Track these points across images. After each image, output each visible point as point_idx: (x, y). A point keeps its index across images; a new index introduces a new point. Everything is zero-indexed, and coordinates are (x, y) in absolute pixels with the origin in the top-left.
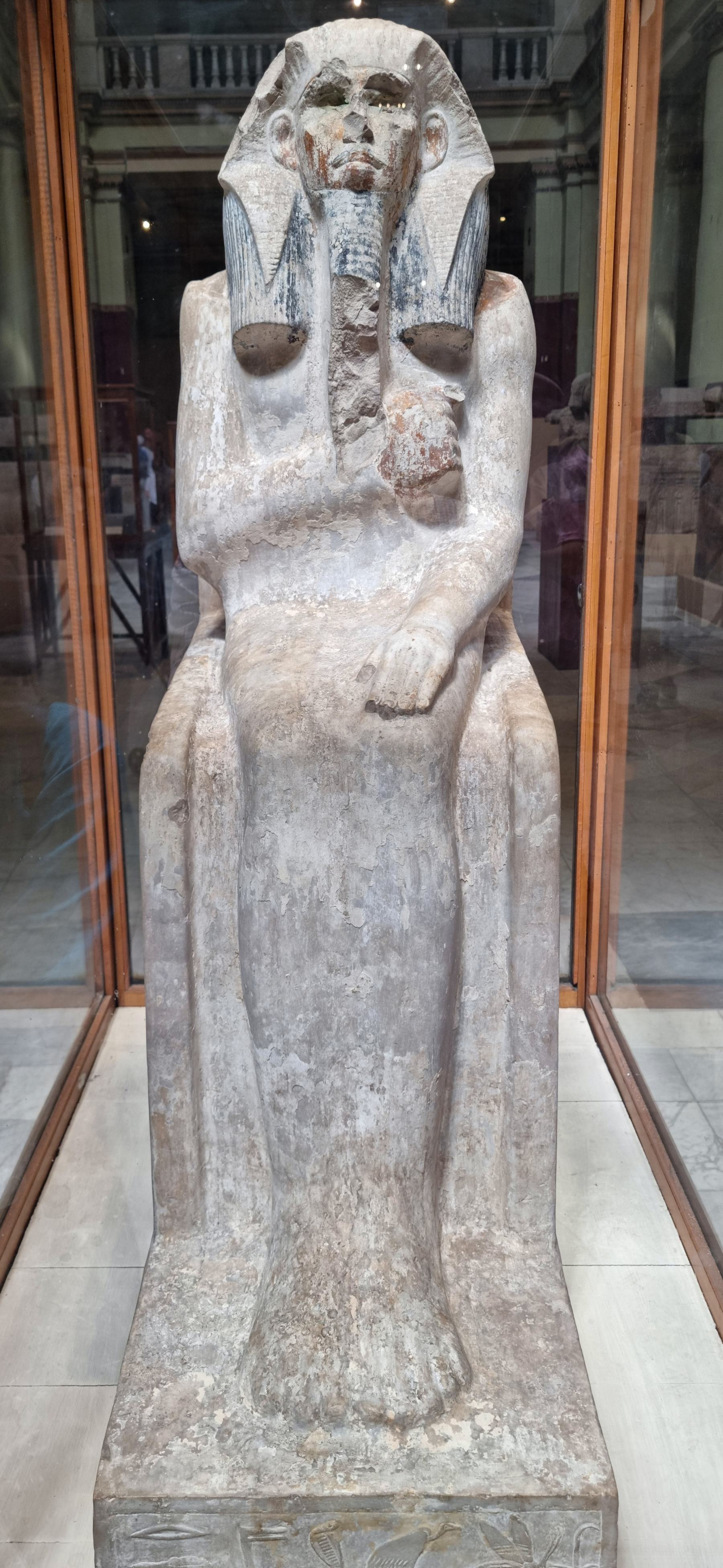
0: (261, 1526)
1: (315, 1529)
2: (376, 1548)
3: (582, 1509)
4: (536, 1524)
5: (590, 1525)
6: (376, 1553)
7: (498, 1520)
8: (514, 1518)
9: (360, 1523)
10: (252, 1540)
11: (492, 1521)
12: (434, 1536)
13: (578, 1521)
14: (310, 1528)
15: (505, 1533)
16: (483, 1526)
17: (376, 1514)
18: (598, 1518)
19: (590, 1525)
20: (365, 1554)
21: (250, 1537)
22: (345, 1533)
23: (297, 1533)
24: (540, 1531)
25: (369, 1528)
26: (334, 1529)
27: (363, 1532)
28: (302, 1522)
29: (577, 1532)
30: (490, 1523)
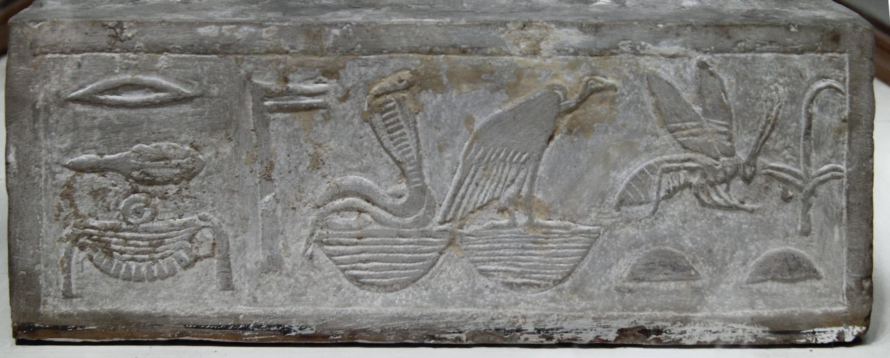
0: (286, 80)
1: (376, 88)
2: (477, 126)
3: (813, 50)
4: (741, 78)
5: (829, 82)
6: (476, 137)
7: (677, 70)
8: (703, 65)
9: (450, 75)
10: (271, 110)
11: (667, 71)
12: (572, 101)
13: (809, 74)
14: (369, 84)
15: (688, 95)
16: (651, 80)
17: (476, 59)
18: (841, 67)
19: (829, 82)
20: (458, 140)
21: (268, 103)
22: (425, 97)
23: (345, 98)
24: (746, 94)
25: (465, 87)
26: (407, 88)
27: (454, 93)
28: (353, 72)
29: (808, 95)
30: (663, 75)
